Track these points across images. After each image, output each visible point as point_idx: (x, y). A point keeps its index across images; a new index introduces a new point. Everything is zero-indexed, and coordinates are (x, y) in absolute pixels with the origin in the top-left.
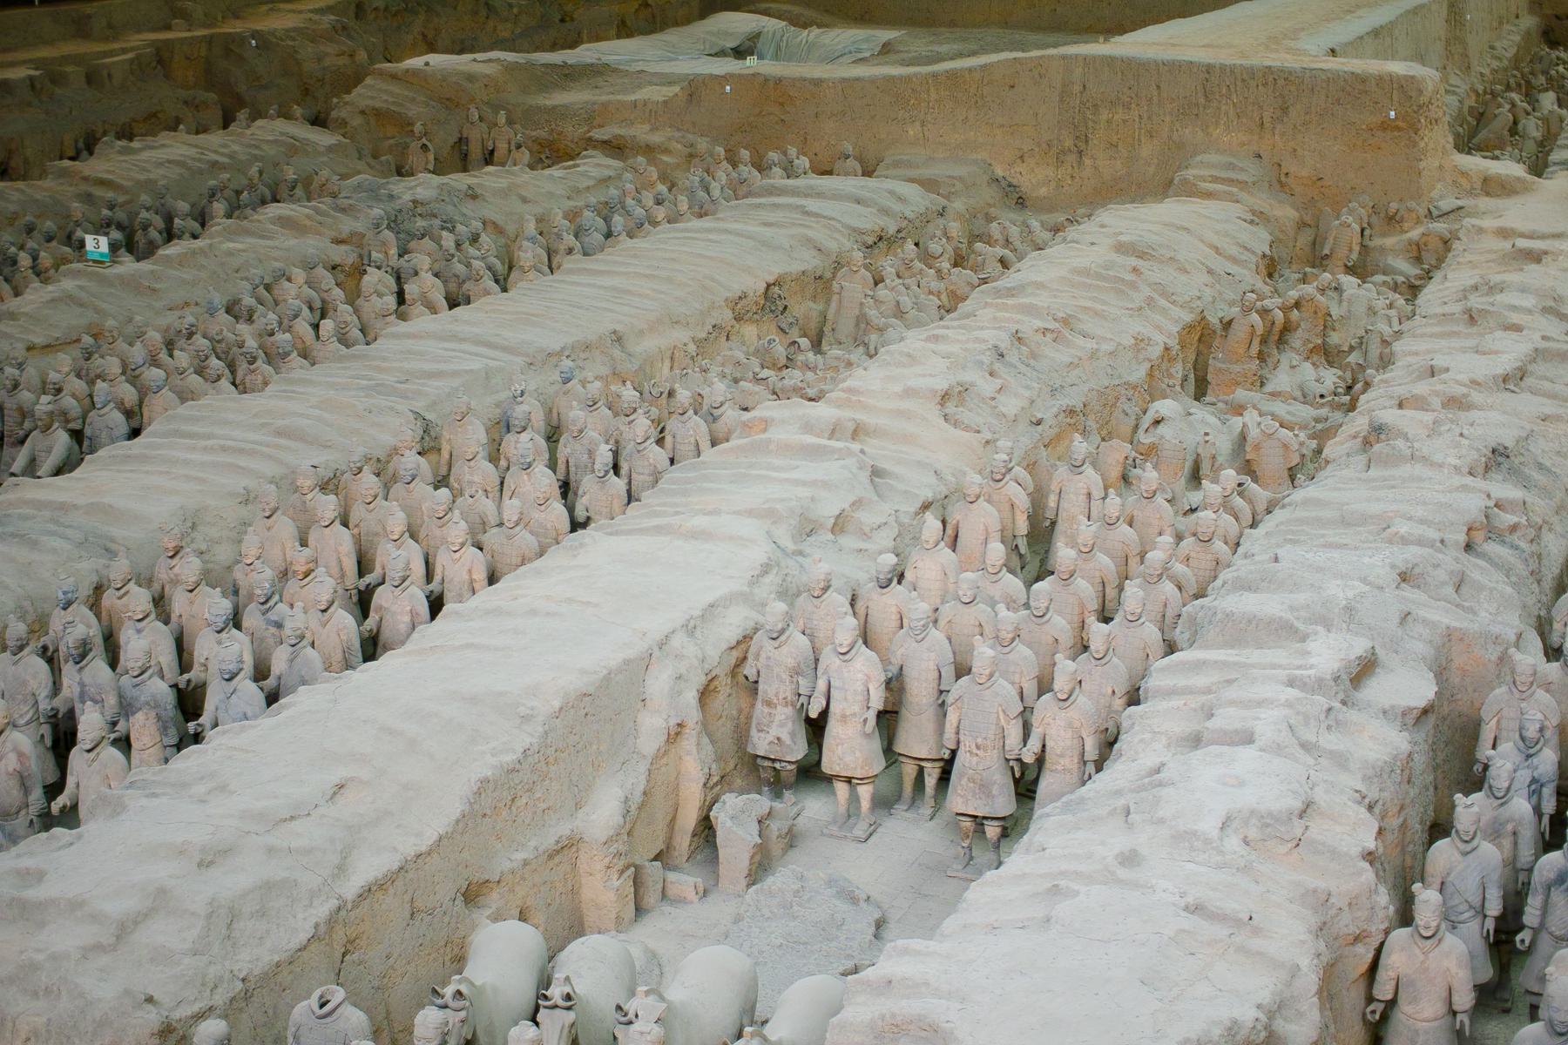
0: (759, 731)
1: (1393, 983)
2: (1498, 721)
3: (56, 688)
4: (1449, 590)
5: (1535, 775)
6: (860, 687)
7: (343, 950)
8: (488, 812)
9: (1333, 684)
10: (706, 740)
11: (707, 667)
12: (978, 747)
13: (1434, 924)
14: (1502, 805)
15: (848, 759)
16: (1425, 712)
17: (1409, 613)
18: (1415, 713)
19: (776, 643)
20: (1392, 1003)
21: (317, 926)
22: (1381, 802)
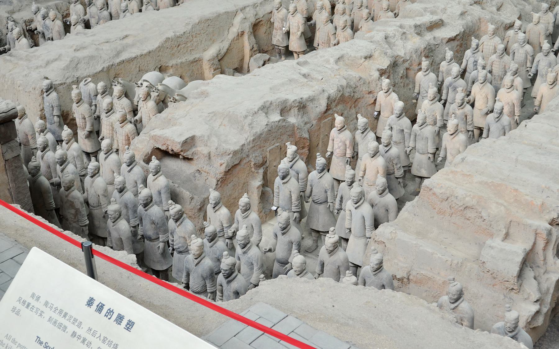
0: (274, 37)
1: (379, 106)
2: (483, 46)
3: (85, 14)
4: (494, 9)
5: (475, 59)
6: (296, 25)
7: (114, 76)
8: (169, 47)
9: (413, 27)
10: (252, 38)
11: (257, 17)
12: (323, 43)
13: (386, 89)
14: (449, 65)
15: (295, 46)
16: (450, 40)
17: (466, 12)
18: (447, 40)
19: (277, 11)
20: (379, 113)
21: (103, 68)
22: (409, 62)
